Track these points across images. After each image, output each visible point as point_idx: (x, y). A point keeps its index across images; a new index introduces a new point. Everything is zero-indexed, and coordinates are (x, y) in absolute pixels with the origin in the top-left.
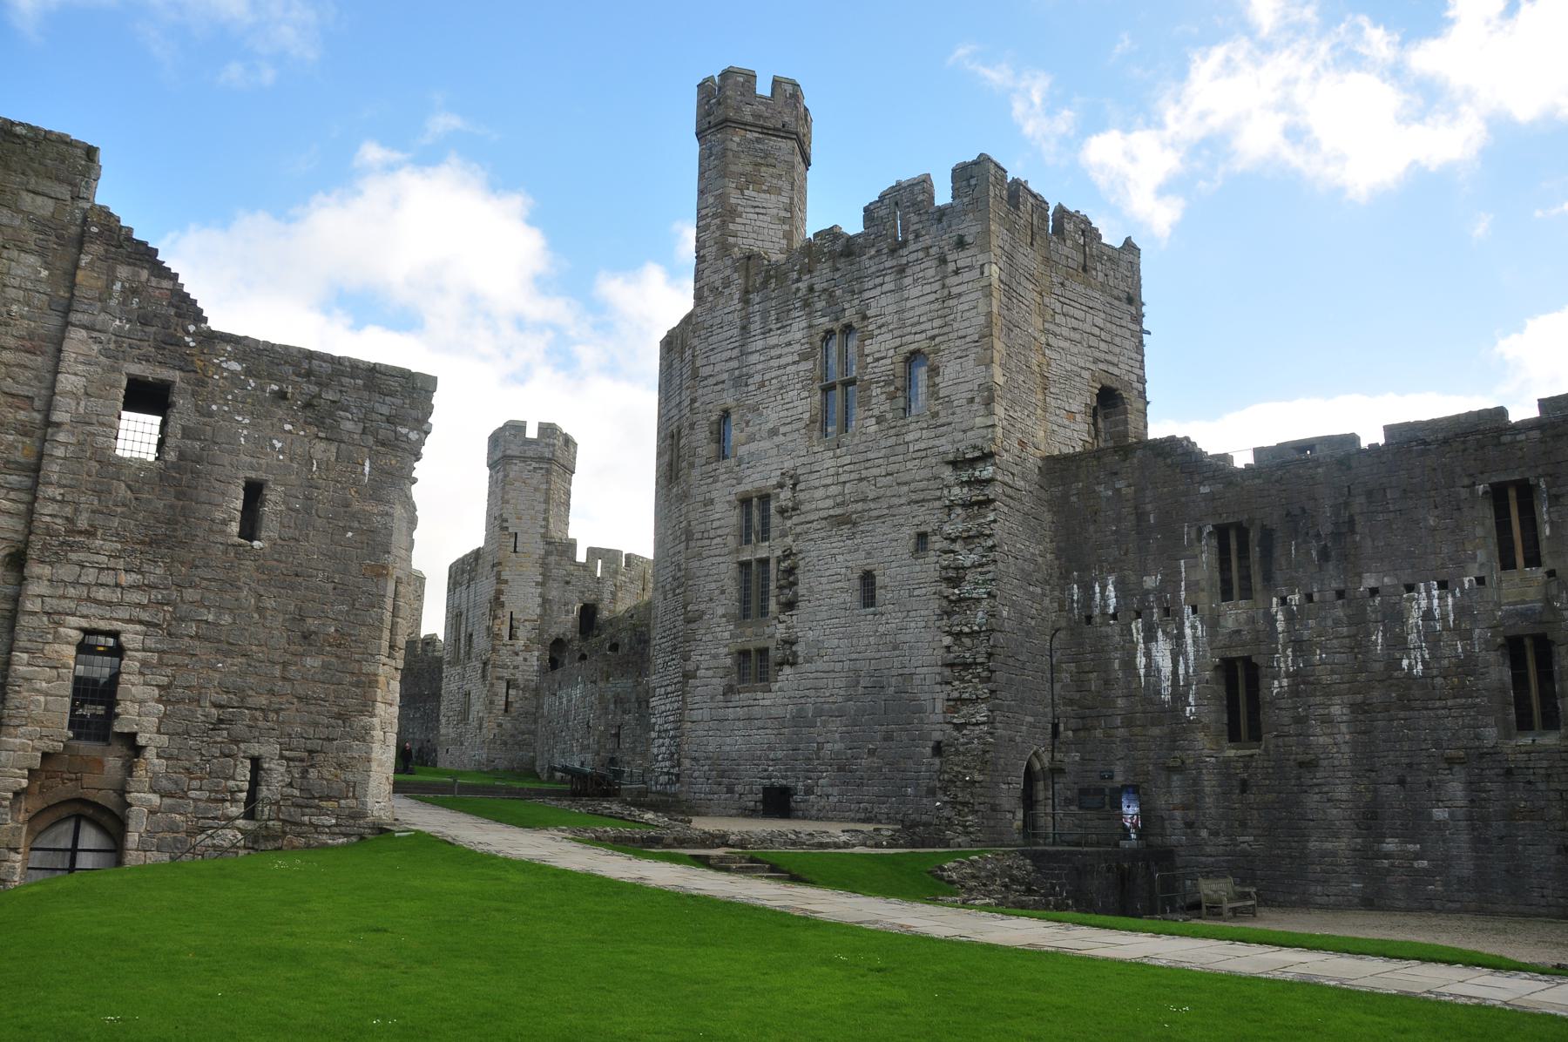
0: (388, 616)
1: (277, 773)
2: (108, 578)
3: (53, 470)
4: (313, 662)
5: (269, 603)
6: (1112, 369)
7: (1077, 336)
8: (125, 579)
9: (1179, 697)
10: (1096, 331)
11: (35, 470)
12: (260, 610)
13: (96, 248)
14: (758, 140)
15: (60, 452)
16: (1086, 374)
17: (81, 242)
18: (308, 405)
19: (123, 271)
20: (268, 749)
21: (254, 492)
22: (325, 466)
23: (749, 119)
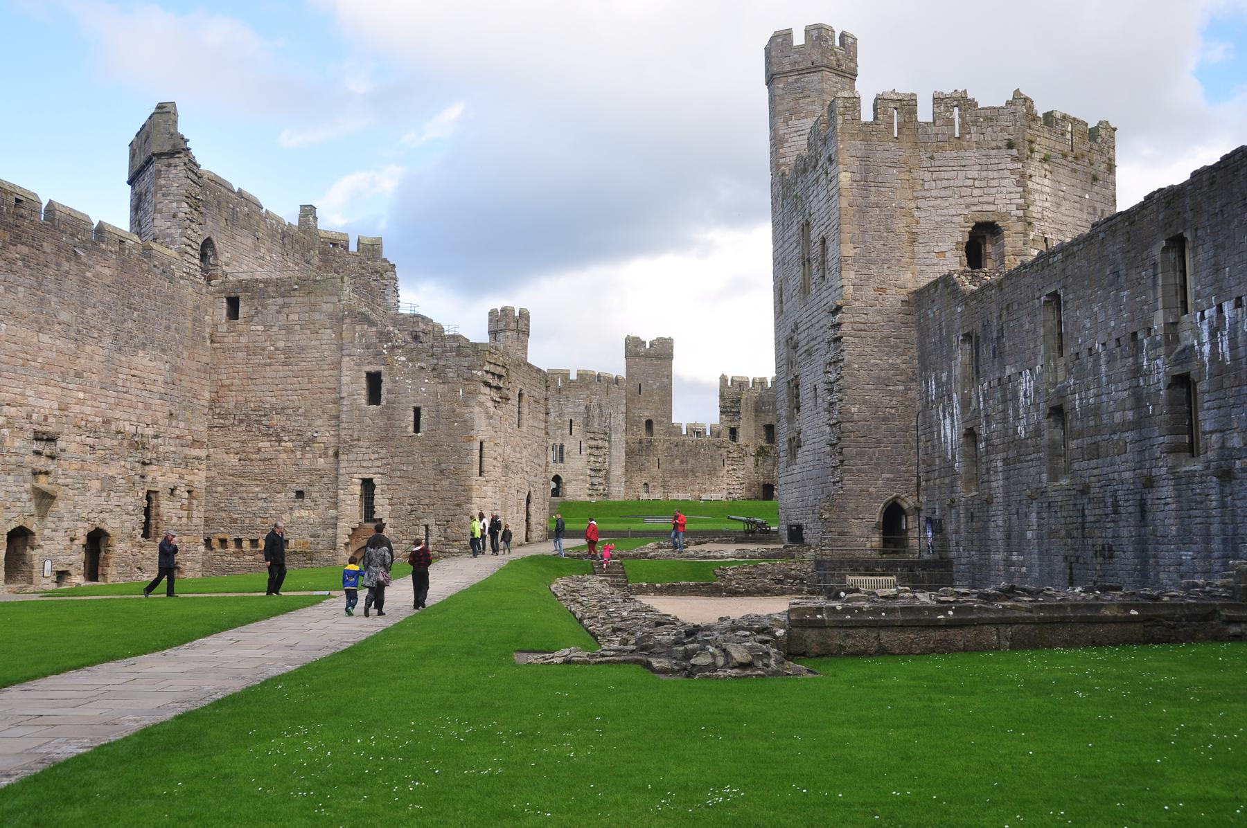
0: (477, 458)
1: (434, 530)
2: (366, 457)
3: (344, 416)
4: (445, 483)
5: (426, 459)
6: (986, 208)
7: (949, 193)
8: (373, 456)
9: (954, 457)
10: (970, 182)
11: (338, 417)
12: (423, 463)
13: (348, 321)
14: (796, 81)
15: (345, 409)
16: (960, 219)
17: (343, 319)
18: (434, 369)
19: (358, 328)
20: (431, 521)
21: (417, 411)
22: (443, 395)
23: (788, 68)
